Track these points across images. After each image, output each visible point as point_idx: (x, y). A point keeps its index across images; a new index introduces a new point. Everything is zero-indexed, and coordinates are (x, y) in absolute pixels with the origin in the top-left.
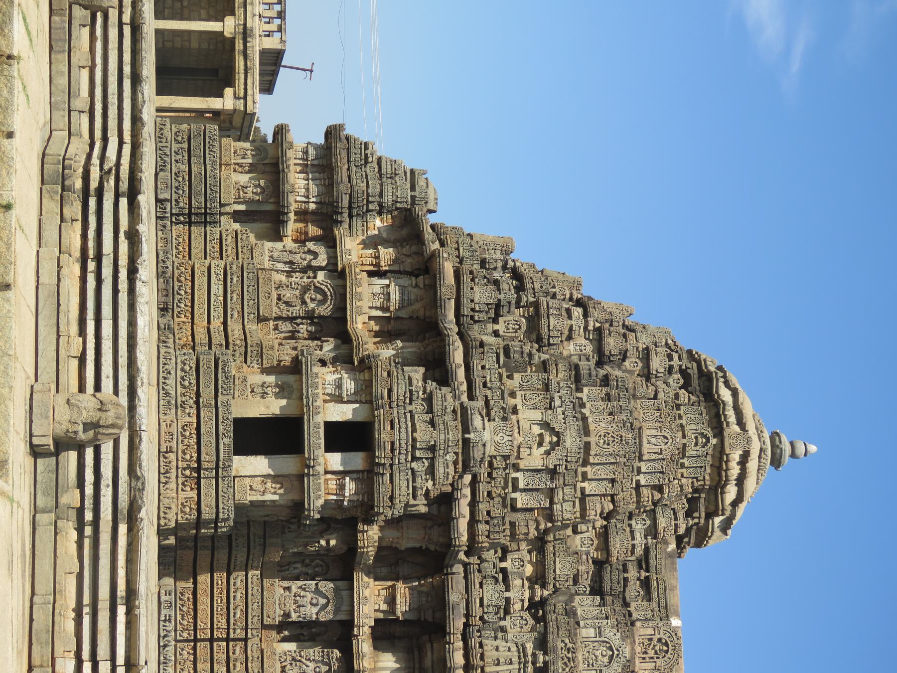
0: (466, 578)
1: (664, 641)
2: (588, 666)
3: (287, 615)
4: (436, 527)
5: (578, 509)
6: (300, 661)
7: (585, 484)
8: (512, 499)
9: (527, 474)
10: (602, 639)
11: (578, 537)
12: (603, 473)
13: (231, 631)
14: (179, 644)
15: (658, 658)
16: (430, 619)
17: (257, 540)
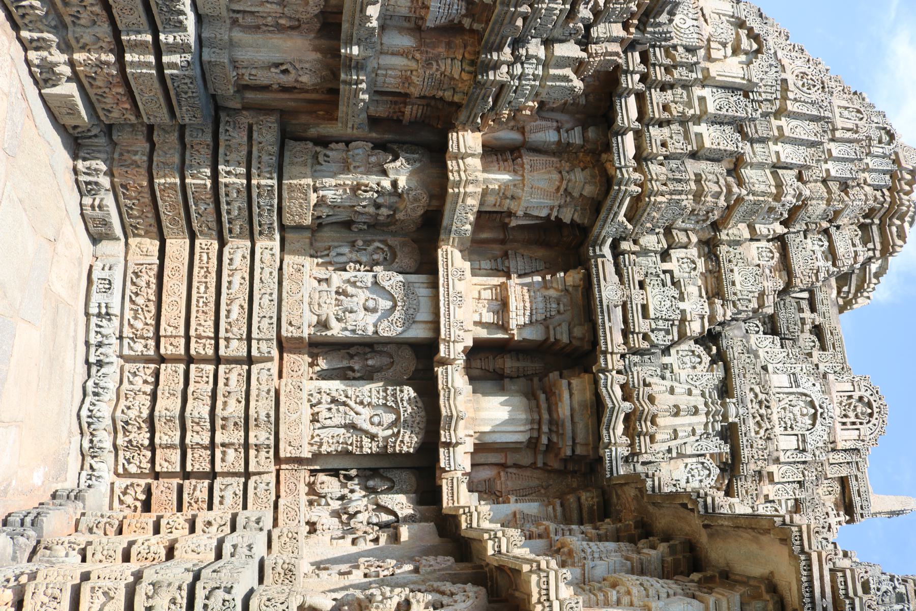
0: (619, 272)
1: (866, 400)
2: (786, 429)
3: (324, 325)
4: (578, 170)
5: (773, 183)
6: (344, 404)
7: (779, 147)
8: (696, 134)
9: (720, 93)
10: (800, 390)
11: (755, 245)
12: (804, 130)
13: (222, 343)
14: (128, 366)
15: (861, 424)
16: (565, 339)
17: (265, 158)
